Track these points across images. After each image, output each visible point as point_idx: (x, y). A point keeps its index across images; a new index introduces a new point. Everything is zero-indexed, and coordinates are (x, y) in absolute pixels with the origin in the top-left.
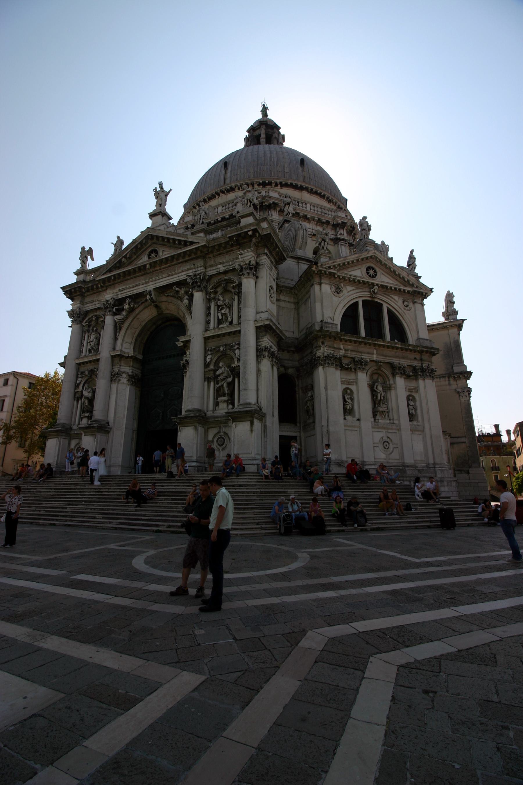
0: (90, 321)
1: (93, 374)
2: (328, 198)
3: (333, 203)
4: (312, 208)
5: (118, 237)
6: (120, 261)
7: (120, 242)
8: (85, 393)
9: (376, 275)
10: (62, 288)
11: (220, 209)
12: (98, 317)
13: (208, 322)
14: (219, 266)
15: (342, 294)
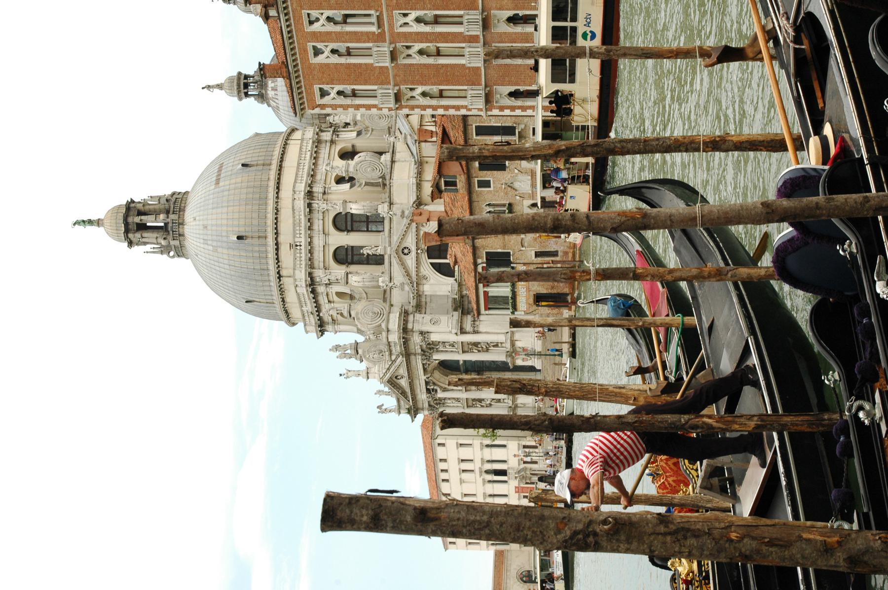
0: (437, 404)
1: (474, 400)
2: (276, 214)
3: (277, 205)
4: (298, 236)
5: (376, 394)
6: (401, 394)
7: (380, 392)
8: (488, 402)
9: (408, 248)
10: (413, 421)
11: (303, 308)
12: (436, 400)
13: (452, 351)
14: (416, 348)
15: (427, 275)
